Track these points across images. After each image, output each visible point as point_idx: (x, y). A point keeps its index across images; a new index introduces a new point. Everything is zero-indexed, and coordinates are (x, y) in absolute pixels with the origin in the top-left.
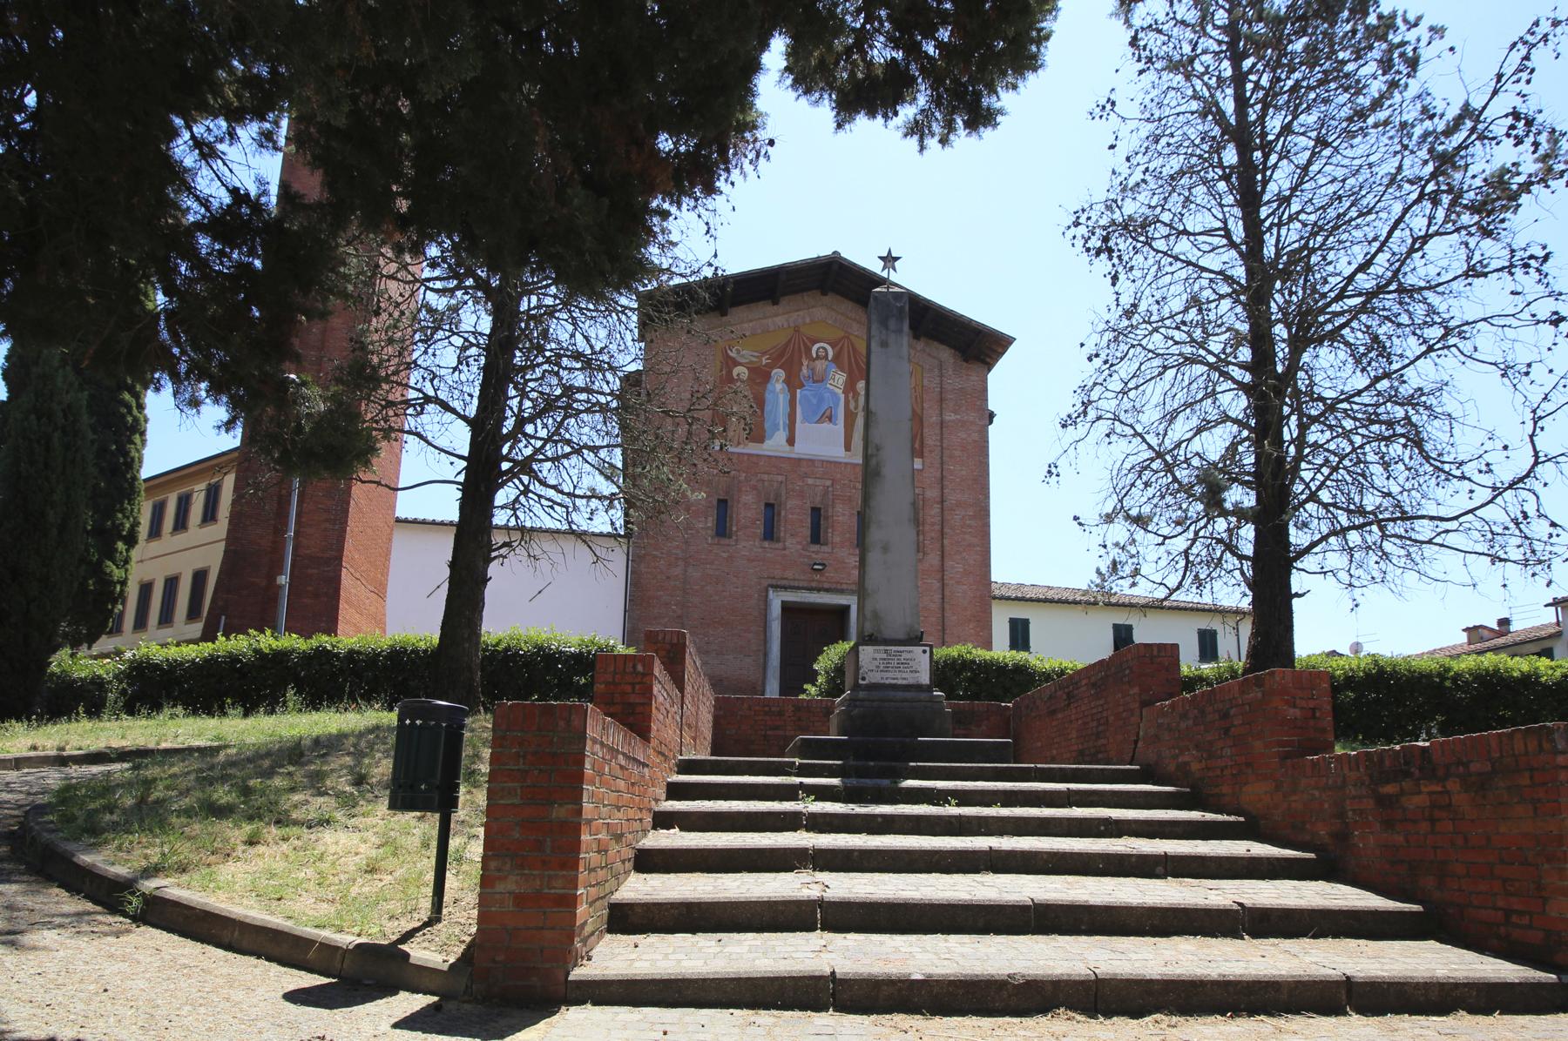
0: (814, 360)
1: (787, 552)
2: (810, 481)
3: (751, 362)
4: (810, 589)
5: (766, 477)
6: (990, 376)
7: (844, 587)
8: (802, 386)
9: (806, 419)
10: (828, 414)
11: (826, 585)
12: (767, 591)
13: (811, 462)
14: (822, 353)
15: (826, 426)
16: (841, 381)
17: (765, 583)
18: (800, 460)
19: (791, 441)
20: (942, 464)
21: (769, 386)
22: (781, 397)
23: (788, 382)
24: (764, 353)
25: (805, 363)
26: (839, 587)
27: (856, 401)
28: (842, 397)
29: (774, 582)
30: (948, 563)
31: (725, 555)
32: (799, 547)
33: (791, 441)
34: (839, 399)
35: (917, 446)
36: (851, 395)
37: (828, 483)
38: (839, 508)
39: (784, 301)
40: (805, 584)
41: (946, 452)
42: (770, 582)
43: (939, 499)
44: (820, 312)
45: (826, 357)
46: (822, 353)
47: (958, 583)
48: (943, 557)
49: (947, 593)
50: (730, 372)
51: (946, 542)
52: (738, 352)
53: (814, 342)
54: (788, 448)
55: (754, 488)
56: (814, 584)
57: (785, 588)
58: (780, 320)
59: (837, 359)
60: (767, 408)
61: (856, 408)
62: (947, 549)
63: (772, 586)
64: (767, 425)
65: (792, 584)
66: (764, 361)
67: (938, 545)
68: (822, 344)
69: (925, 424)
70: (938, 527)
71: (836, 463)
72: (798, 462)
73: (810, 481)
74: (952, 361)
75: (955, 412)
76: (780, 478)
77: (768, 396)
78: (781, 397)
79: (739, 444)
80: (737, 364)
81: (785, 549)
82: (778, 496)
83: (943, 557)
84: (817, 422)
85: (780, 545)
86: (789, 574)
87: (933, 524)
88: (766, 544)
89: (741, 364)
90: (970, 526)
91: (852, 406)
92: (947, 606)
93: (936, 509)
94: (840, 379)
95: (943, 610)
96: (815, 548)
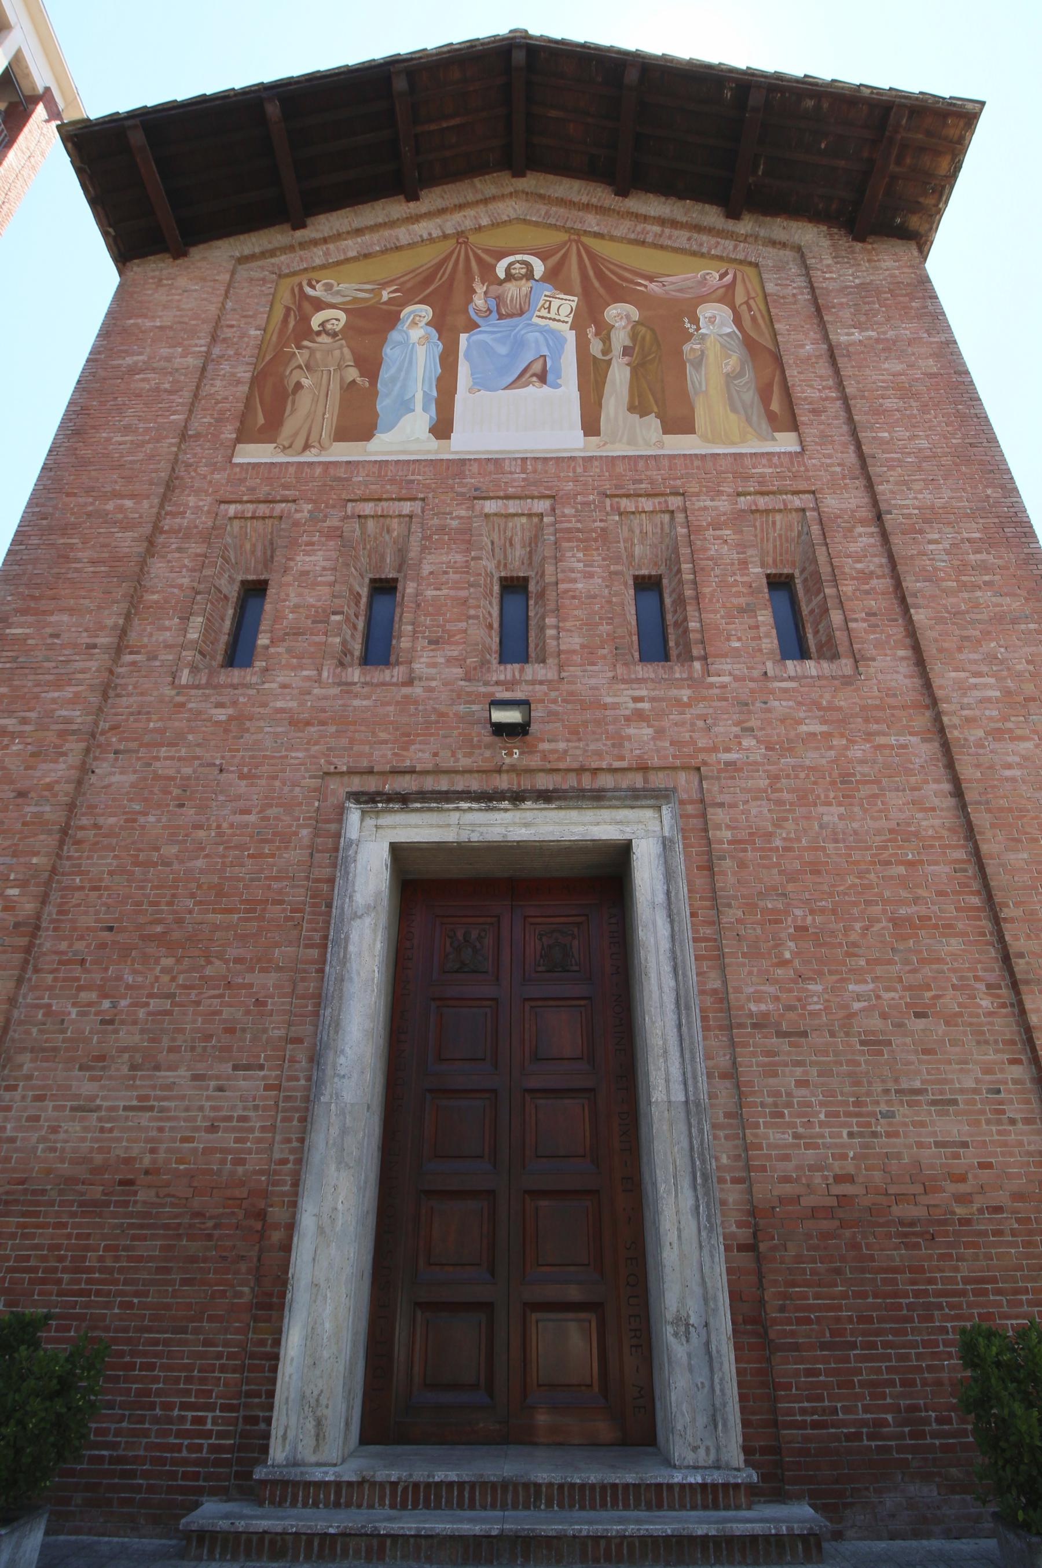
0: (501, 282)
1: (417, 690)
2: (490, 507)
3: (355, 300)
4: (488, 798)
5: (368, 508)
6: (927, 265)
7: (606, 781)
8: (471, 326)
9: (480, 384)
10: (537, 367)
11: (543, 782)
12: (340, 813)
13: (495, 464)
14: (519, 270)
15: (534, 391)
16: (565, 310)
17: (338, 788)
18: (463, 462)
19: (442, 428)
20: (854, 433)
21: (394, 336)
22: (421, 352)
23: (438, 324)
24: (384, 285)
25: (480, 289)
26: (586, 782)
27: (607, 340)
28: (571, 336)
29: (371, 784)
30: (945, 678)
31: (221, 715)
32: (458, 672)
33: (442, 428)
34: (560, 341)
35: (775, 406)
36: (591, 331)
37: (542, 506)
38: (574, 560)
39: (431, 199)
40: (475, 784)
41: (859, 406)
42: (356, 784)
43: (866, 513)
44: (508, 209)
45: (529, 275)
46: (519, 270)
47: (997, 734)
48: (920, 662)
49: (967, 771)
50: (305, 320)
51: (919, 616)
52: (328, 287)
53: (501, 255)
54: (433, 444)
55: (336, 534)
56: (503, 782)
57: (403, 800)
58: (423, 228)
59: (553, 276)
60: (385, 374)
61: (607, 351)
62: (929, 636)
63: (357, 797)
64: (383, 405)
65: (429, 784)
66: (385, 295)
67: (897, 631)
68: (519, 257)
69: (788, 359)
70: (883, 584)
71: (558, 460)
72: (460, 466)
73: (490, 507)
74: (826, 243)
75: (859, 326)
76: (407, 507)
77: (390, 352)
78: (421, 352)
79: (306, 447)
80: (319, 305)
81: (410, 682)
82: (402, 553)
83: (920, 662)
84: (508, 387)
85: (398, 673)
86: (420, 756)
87: (866, 576)
88: (355, 674)
89: (333, 306)
90: (984, 568)
91: (596, 347)
92: (981, 818)
93: (865, 538)
94: (565, 306)
95: (970, 832)
96: (511, 670)
